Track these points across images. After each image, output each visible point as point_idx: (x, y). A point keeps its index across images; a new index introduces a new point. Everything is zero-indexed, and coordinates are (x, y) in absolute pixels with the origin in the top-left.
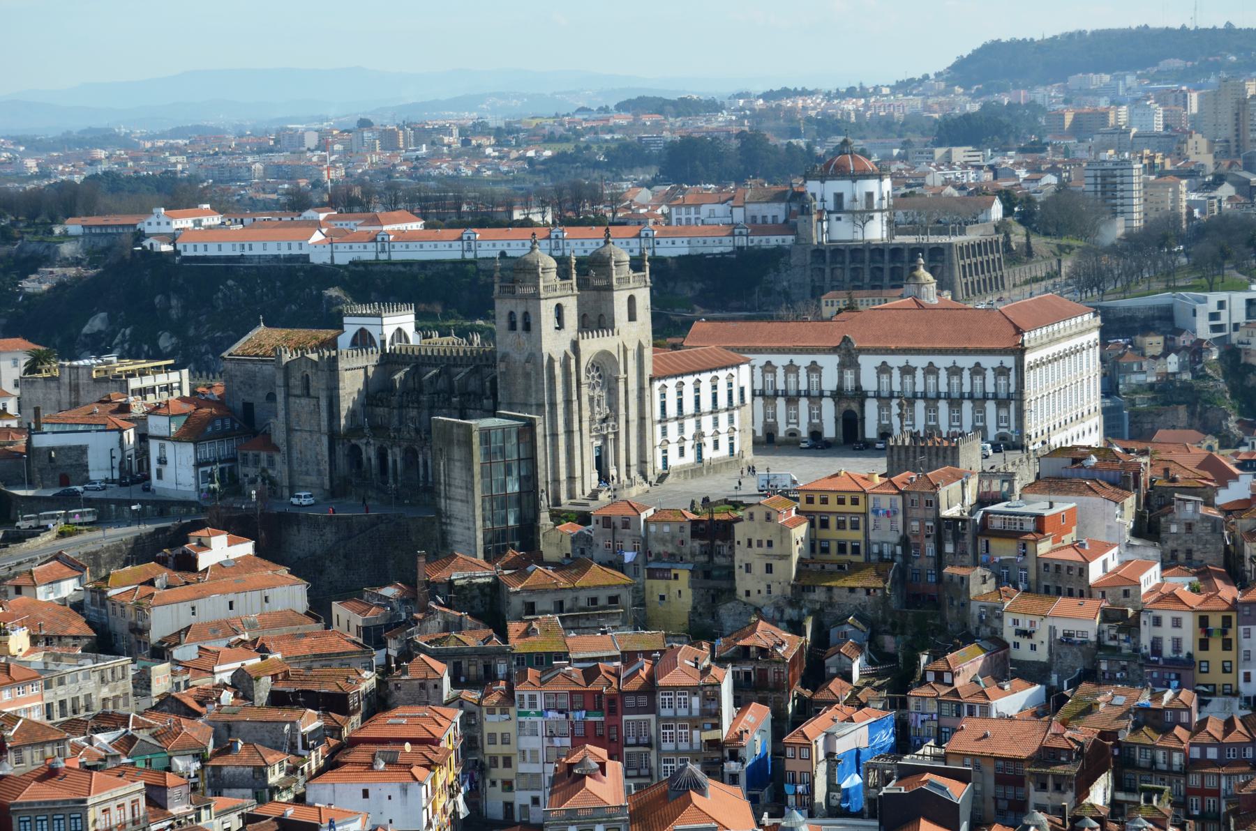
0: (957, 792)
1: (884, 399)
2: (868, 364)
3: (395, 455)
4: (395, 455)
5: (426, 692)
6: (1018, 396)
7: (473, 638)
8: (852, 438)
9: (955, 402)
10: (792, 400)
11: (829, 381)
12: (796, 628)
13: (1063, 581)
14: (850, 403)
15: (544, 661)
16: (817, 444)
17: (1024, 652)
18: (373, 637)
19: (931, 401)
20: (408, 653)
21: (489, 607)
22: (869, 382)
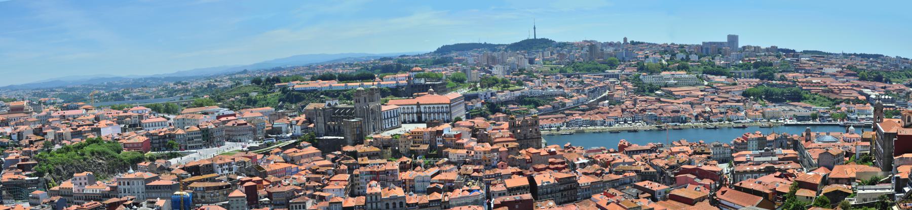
0: (442, 186)
1: (425, 113)
2: (422, 107)
3: (336, 128)
4: (336, 128)
5: (343, 172)
6: (449, 113)
7: (352, 161)
8: (420, 121)
9: (438, 113)
10: (409, 114)
11: (415, 110)
12: (410, 157)
13: (461, 146)
14: (419, 113)
15: (364, 165)
16: (413, 122)
17: (453, 160)
18: (333, 160)
19: (434, 113)
20: (340, 164)
21: (355, 155)
22: (422, 110)
